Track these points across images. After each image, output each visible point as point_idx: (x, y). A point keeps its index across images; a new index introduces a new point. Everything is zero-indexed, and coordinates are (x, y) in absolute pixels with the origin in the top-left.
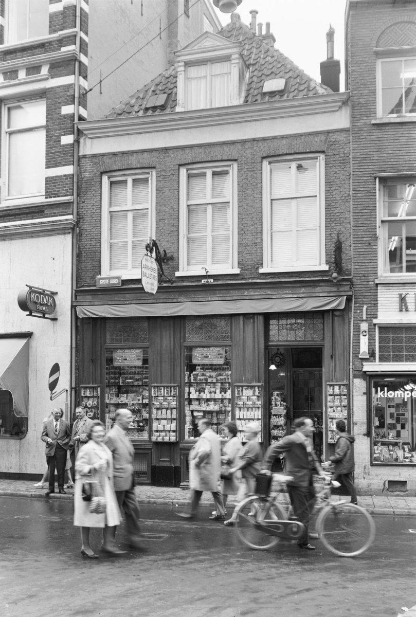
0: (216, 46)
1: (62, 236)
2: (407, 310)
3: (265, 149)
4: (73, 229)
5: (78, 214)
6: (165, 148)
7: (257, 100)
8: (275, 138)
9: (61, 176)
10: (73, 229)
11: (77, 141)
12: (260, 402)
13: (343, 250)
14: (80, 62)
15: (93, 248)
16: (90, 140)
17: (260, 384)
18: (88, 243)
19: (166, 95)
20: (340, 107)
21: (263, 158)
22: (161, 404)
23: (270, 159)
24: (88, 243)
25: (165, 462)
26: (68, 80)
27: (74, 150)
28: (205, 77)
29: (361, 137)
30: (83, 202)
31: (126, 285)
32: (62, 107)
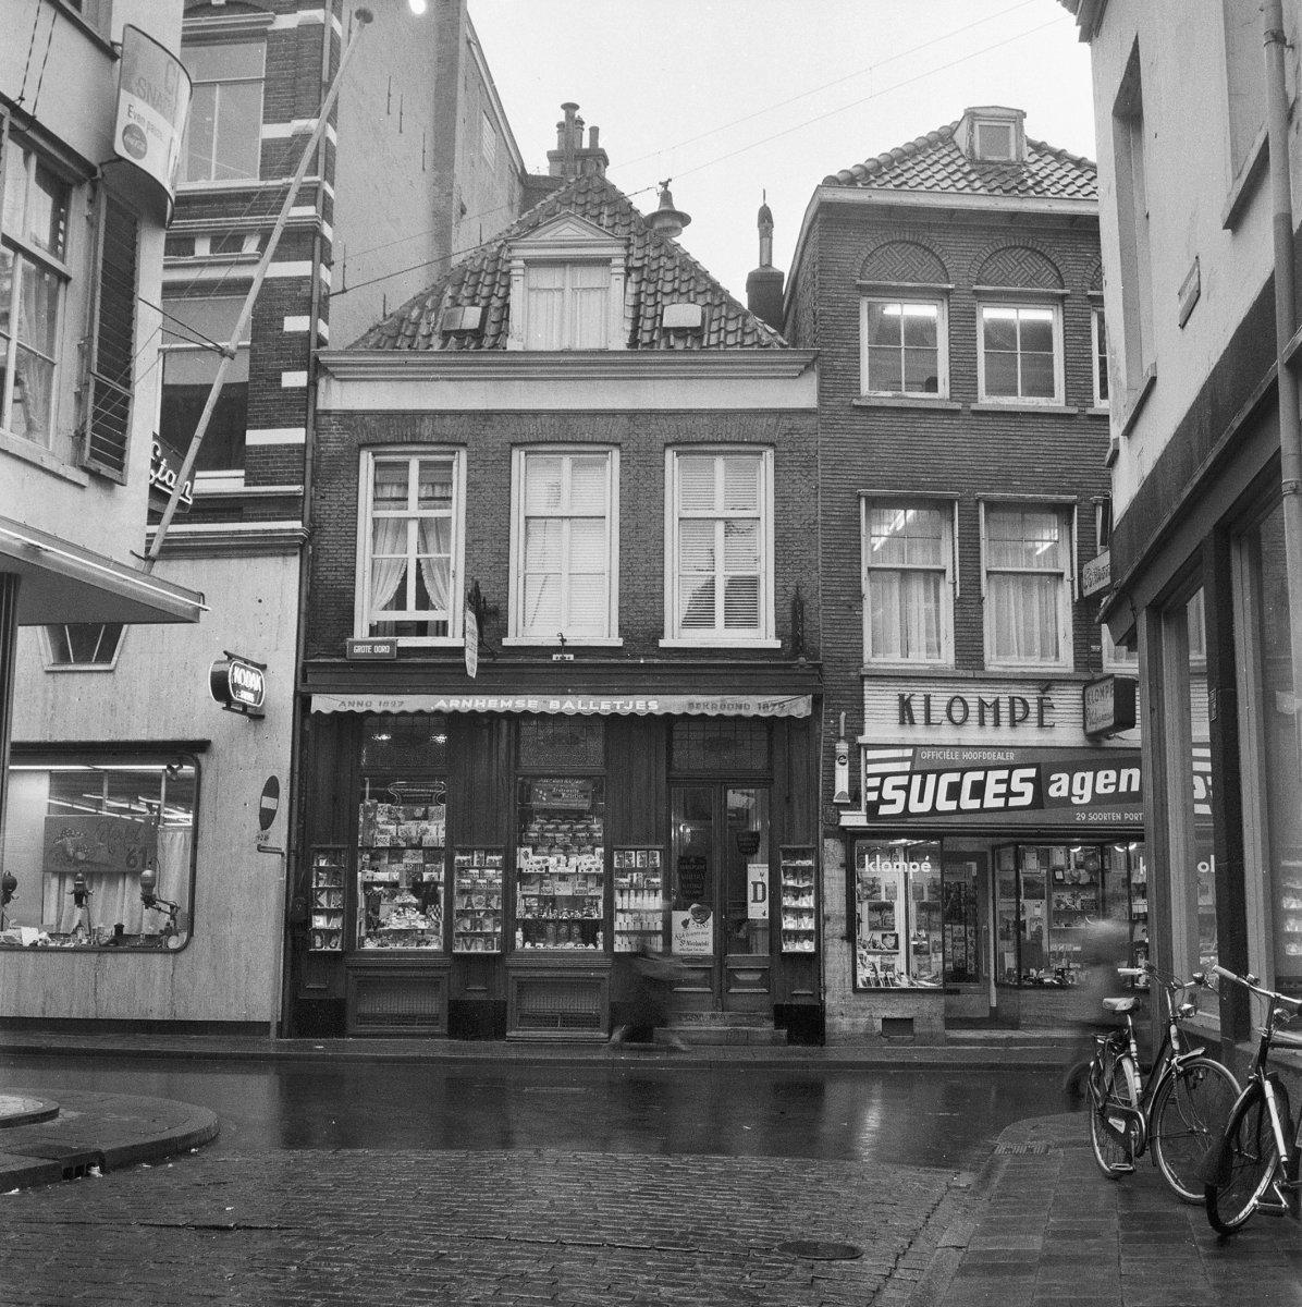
0: (583, 240)
1: (280, 560)
2: (912, 722)
3: (669, 430)
4: (302, 547)
5: (312, 520)
6: (487, 410)
7: (652, 342)
8: (689, 412)
9: (280, 446)
10: (302, 547)
11: (313, 383)
12: (658, 880)
13: (806, 615)
14: (323, 238)
15: (339, 584)
16: (338, 383)
17: (662, 847)
18: (331, 575)
19: (478, 310)
20: (801, 373)
21: (667, 445)
22: (474, 882)
23: (680, 449)
24: (331, 575)
25: (477, 993)
26: (302, 268)
27: (307, 400)
28: (561, 290)
29: (836, 426)
30: (322, 497)
31: (403, 656)
32: (286, 318)
